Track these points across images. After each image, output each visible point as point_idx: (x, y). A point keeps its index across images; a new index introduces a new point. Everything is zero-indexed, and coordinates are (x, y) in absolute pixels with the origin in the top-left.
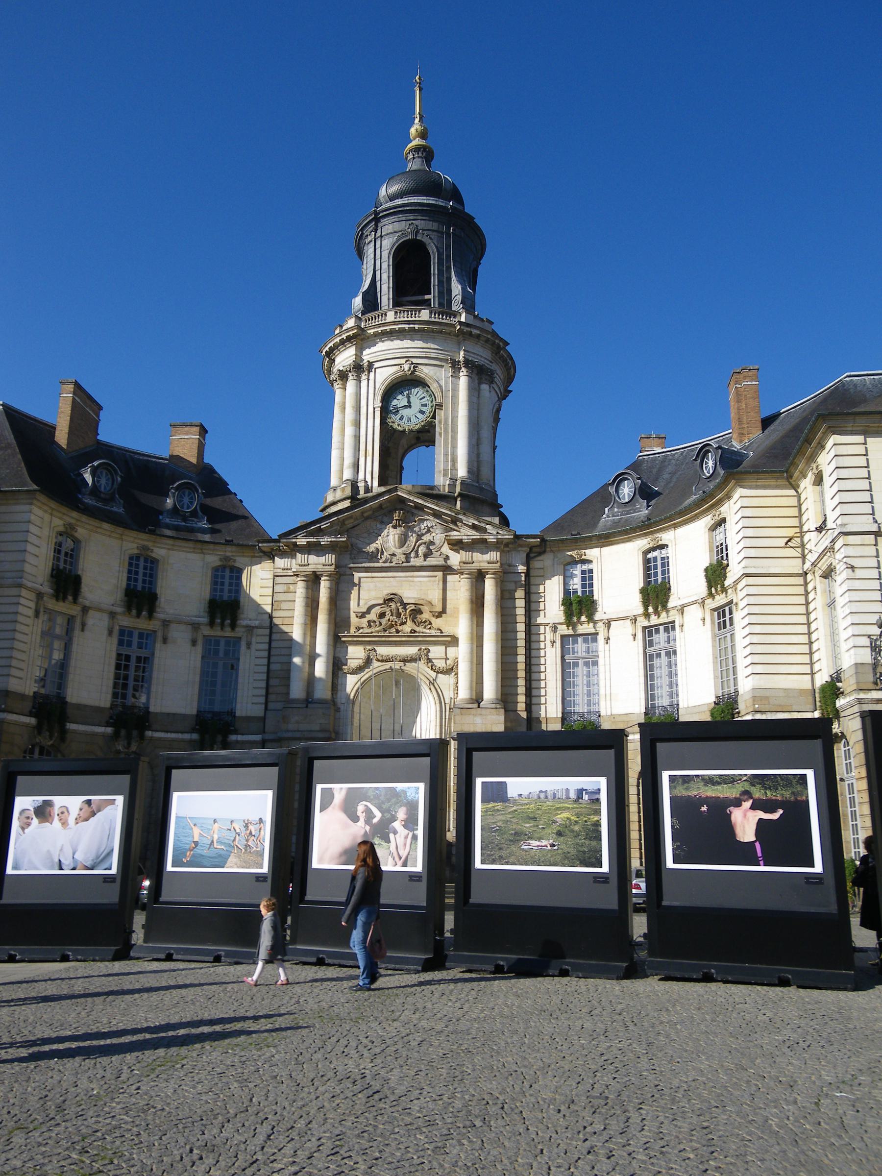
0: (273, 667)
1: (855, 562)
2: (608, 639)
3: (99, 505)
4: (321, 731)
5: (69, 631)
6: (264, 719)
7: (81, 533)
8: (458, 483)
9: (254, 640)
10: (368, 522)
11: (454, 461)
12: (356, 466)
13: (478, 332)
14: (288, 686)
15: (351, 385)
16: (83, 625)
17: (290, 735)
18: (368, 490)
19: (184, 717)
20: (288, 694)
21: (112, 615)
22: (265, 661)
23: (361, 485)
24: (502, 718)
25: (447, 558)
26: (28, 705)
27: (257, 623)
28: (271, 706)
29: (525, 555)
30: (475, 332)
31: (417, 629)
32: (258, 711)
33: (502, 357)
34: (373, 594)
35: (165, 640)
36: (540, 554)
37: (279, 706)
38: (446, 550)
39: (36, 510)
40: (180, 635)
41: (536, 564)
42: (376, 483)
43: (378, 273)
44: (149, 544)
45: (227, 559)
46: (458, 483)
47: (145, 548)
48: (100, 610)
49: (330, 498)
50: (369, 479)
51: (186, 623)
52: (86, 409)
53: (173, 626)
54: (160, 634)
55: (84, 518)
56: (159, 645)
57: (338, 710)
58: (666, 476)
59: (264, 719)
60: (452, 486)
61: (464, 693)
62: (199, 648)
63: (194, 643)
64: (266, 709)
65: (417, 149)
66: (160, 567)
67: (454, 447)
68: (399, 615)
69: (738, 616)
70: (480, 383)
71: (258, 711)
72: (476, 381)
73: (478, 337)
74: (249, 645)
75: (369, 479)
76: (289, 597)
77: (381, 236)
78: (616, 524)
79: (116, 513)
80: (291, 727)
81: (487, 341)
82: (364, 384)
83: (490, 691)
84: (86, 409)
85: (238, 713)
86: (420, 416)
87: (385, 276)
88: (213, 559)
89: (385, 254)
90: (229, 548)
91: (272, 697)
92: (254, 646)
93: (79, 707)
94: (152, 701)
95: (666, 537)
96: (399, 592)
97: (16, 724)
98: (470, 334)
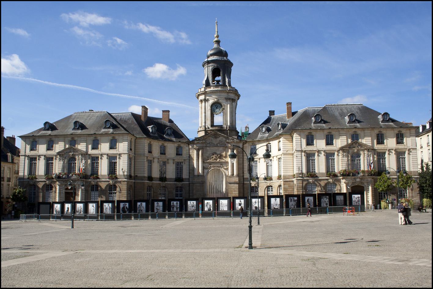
0: (190, 168)
1: (297, 156)
2: (259, 162)
3: (153, 135)
4: (201, 182)
5: (151, 163)
6: (189, 179)
7: (152, 143)
8: (228, 126)
9: (186, 162)
10: (209, 137)
11: (227, 121)
12: (205, 123)
13: (232, 92)
14: (194, 172)
15: (203, 103)
16: (154, 161)
17: (195, 182)
18: (208, 128)
19: (173, 179)
20: (194, 174)
21: (158, 159)
22: (188, 167)
23: (207, 127)
24: (238, 179)
25: (226, 144)
26: (147, 179)
27: (186, 159)
28: (190, 176)
29: (242, 144)
30: (231, 92)
31: (220, 160)
32: (188, 177)
33: (237, 95)
34: (211, 153)
35: (168, 163)
36: (246, 143)
37: (192, 176)
38: (225, 143)
39: (146, 141)
40: (171, 162)
41: (245, 146)
42: (210, 127)
43: (209, 75)
44: (164, 143)
45: (179, 145)
46: (228, 126)
47: (163, 144)
48: (156, 158)
49: (200, 129)
50: (208, 126)
51: (172, 159)
52: (145, 109)
53: (169, 160)
54: (167, 162)
55: (153, 140)
56: (167, 164)
57: (204, 177)
58: (273, 124)
59: (189, 179)
60: (227, 127)
61: (230, 174)
62: (175, 164)
63: (174, 163)
64: (189, 177)
65: (216, 41)
66: (166, 148)
67: (227, 118)
68: (216, 157)
69: (282, 160)
70: (232, 102)
71: (188, 177)
72: (232, 102)
73: (232, 92)
74: (185, 164)
75: (208, 126)
76: (193, 153)
77: (209, 66)
78: (262, 137)
79: (156, 136)
80: (195, 181)
81: (234, 93)
82: (207, 103)
83: (235, 173)
84: (145, 109)
85: (183, 178)
86: (219, 111)
87: (210, 76)
88: (176, 145)
89: (210, 70)
90: (180, 143)
91: (190, 175)
92: (186, 164)
93: (154, 178)
94: (167, 176)
95: (270, 142)
96: (216, 152)
97: (146, 182)
98: (230, 92)
